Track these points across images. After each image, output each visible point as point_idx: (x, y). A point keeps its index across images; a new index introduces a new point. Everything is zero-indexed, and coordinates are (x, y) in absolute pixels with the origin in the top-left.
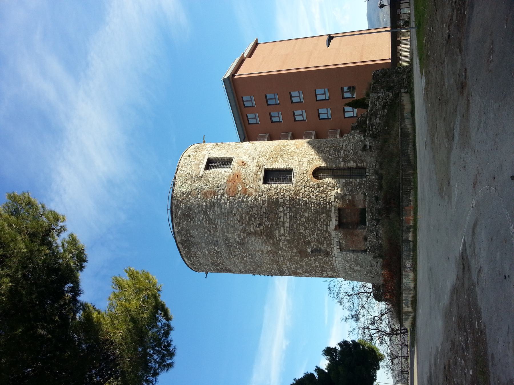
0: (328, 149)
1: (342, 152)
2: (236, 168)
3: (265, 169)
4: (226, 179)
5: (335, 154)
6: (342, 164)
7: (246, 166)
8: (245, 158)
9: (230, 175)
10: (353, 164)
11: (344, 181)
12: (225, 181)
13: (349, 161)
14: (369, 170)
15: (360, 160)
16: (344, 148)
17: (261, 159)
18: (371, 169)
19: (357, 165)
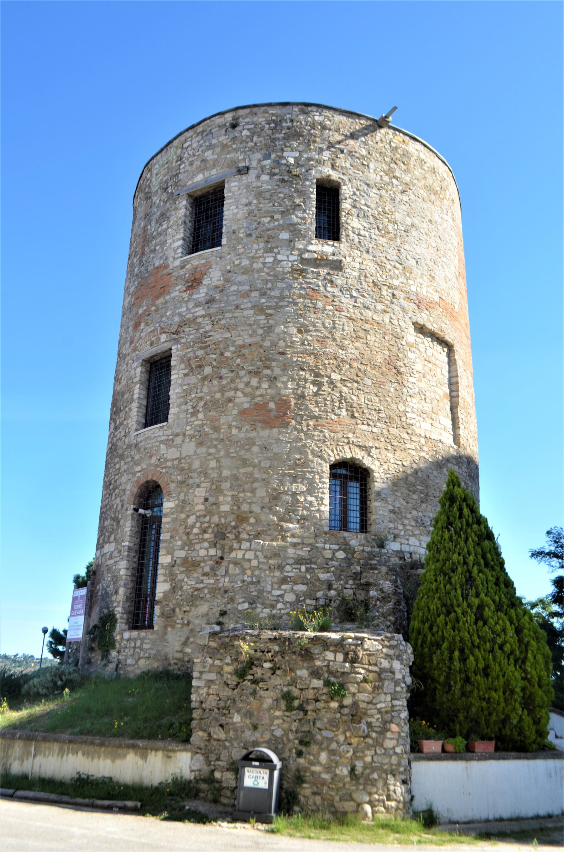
0: (225, 508)
1: (212, 552)
2: (182, 272)
3: (171, 349)
4: (162, 262)
5: (205, 532)
6: (164, 559)
7: (185, 296)
8: (214, 277)
9: (166, 266)
10: (162, 588)
11: (123, 572)
12: (157, 264)
13: (172, 577)
14: (135, 640)
15: (174, 610)
16: (233, 555)
17: (207, 321)
18: (138, 643)
19: (158, 602)
